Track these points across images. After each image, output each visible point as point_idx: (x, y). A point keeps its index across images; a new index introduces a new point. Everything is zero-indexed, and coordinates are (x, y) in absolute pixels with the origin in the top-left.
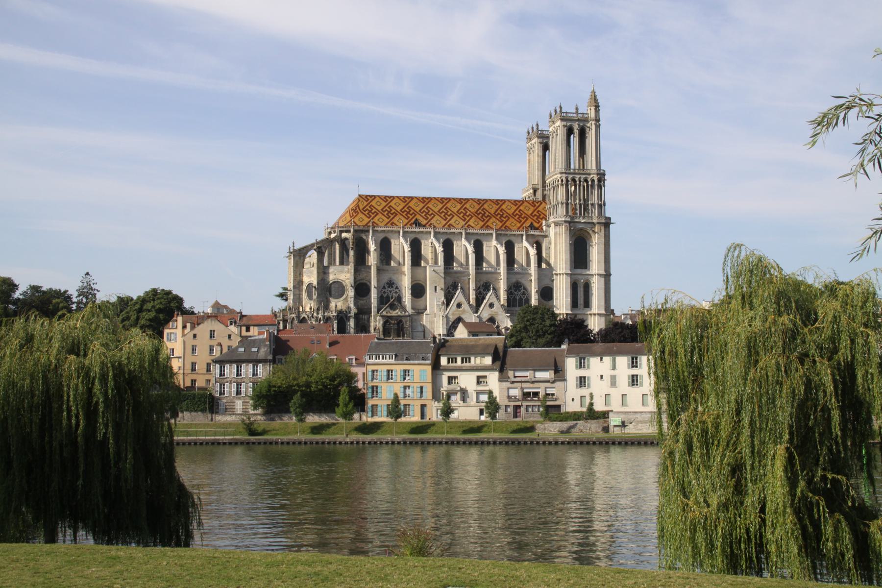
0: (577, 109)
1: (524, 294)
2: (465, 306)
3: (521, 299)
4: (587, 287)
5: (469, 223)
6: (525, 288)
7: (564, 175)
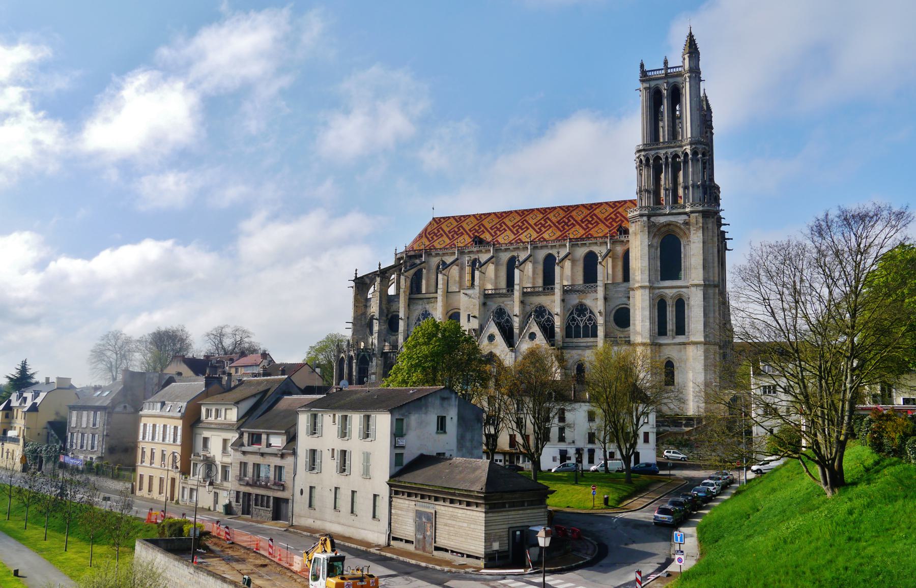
0: (666, 63)
1: (590, 319)
2: (499, 339)
3: (586, 326)
4: (680, 304)
6: (591, 312)
7: (643, 153)
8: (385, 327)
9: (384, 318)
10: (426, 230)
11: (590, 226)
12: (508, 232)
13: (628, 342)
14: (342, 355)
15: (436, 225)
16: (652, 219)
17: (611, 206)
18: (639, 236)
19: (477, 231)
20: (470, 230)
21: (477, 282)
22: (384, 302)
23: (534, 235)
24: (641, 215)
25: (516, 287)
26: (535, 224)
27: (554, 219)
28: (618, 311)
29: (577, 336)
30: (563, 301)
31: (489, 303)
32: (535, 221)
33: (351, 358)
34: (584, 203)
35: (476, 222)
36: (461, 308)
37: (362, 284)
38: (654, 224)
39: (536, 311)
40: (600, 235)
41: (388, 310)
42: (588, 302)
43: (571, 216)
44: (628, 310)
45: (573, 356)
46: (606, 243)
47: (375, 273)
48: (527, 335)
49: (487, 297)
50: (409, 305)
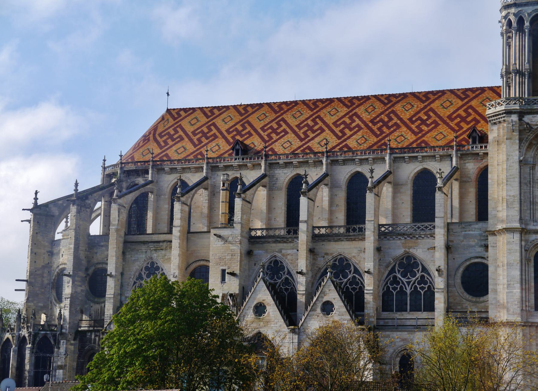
1: (422, 280)
2: (273, 311)
3: (415, 292)
5: (348, 142)
6: (424, 269)
7: (513, 10)
8: (83, 288)
9: (82, 274)
10: (155, 128)
11: (424, 128)
12: (291, 136)
13: (485, 321)
14: (8, 335)
15: (172, 122)
16: (527, 119)
17: (458, 97)
18: (504, 147)
19: (239, 133)
20: (228, 131)
21: (237, 217)
22: (83, 247)
23: (333, 141)
24: (509, 112)
25: (303, 227)
26: (335, 123)
27: (366, 117)
28: (467, 268)
29: (402, 308)
30: (378, 250)
31: (256, 252)
32: (335, 118)
33: (22, 341)
34: (416, 90)
35: (238, 118)
36: (211, 258)
37: (44, 216)
38: (530, 127)
39: (334, 266)
40: (440, 143)
41: (89, 262)
42: (420, 252)
43: (393, 112)
44: (485, 267)
45: (393, 341)
46: (450, 157)
47: (67, 199)
48: (319, 305)
49: (253, 242)
50: (124, 253)
